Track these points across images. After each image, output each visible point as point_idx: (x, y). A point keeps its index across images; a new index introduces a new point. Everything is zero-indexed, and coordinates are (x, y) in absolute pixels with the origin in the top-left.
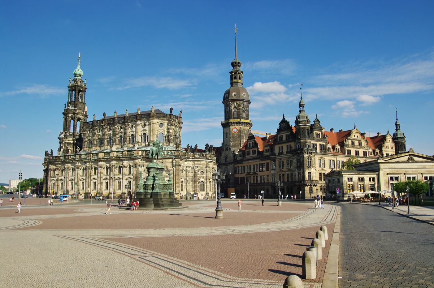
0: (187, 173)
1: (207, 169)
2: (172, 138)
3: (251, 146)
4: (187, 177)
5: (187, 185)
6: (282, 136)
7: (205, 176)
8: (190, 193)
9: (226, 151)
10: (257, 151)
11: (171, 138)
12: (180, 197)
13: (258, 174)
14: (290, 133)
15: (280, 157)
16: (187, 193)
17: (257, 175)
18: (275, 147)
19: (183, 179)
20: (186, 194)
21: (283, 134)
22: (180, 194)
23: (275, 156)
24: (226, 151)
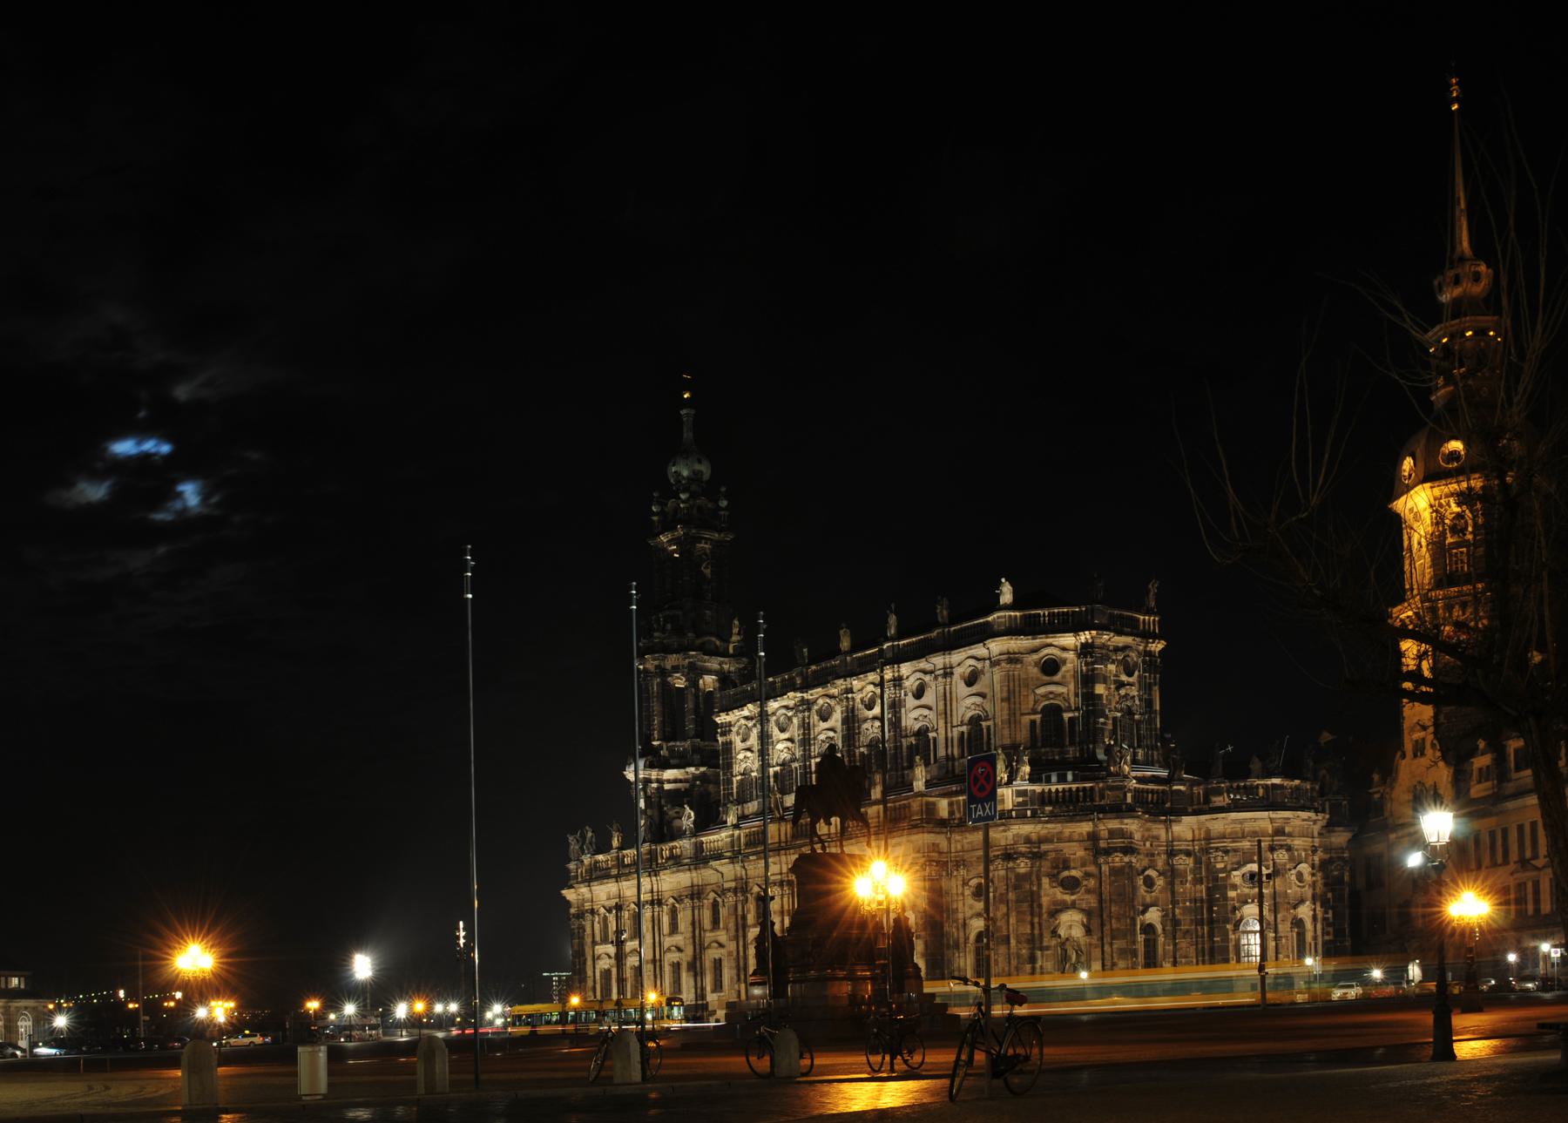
0: (1172, 883)
1: (1281, 856)
4: (1174, 903)
5: (1175, 945)
19: (1153, 916)
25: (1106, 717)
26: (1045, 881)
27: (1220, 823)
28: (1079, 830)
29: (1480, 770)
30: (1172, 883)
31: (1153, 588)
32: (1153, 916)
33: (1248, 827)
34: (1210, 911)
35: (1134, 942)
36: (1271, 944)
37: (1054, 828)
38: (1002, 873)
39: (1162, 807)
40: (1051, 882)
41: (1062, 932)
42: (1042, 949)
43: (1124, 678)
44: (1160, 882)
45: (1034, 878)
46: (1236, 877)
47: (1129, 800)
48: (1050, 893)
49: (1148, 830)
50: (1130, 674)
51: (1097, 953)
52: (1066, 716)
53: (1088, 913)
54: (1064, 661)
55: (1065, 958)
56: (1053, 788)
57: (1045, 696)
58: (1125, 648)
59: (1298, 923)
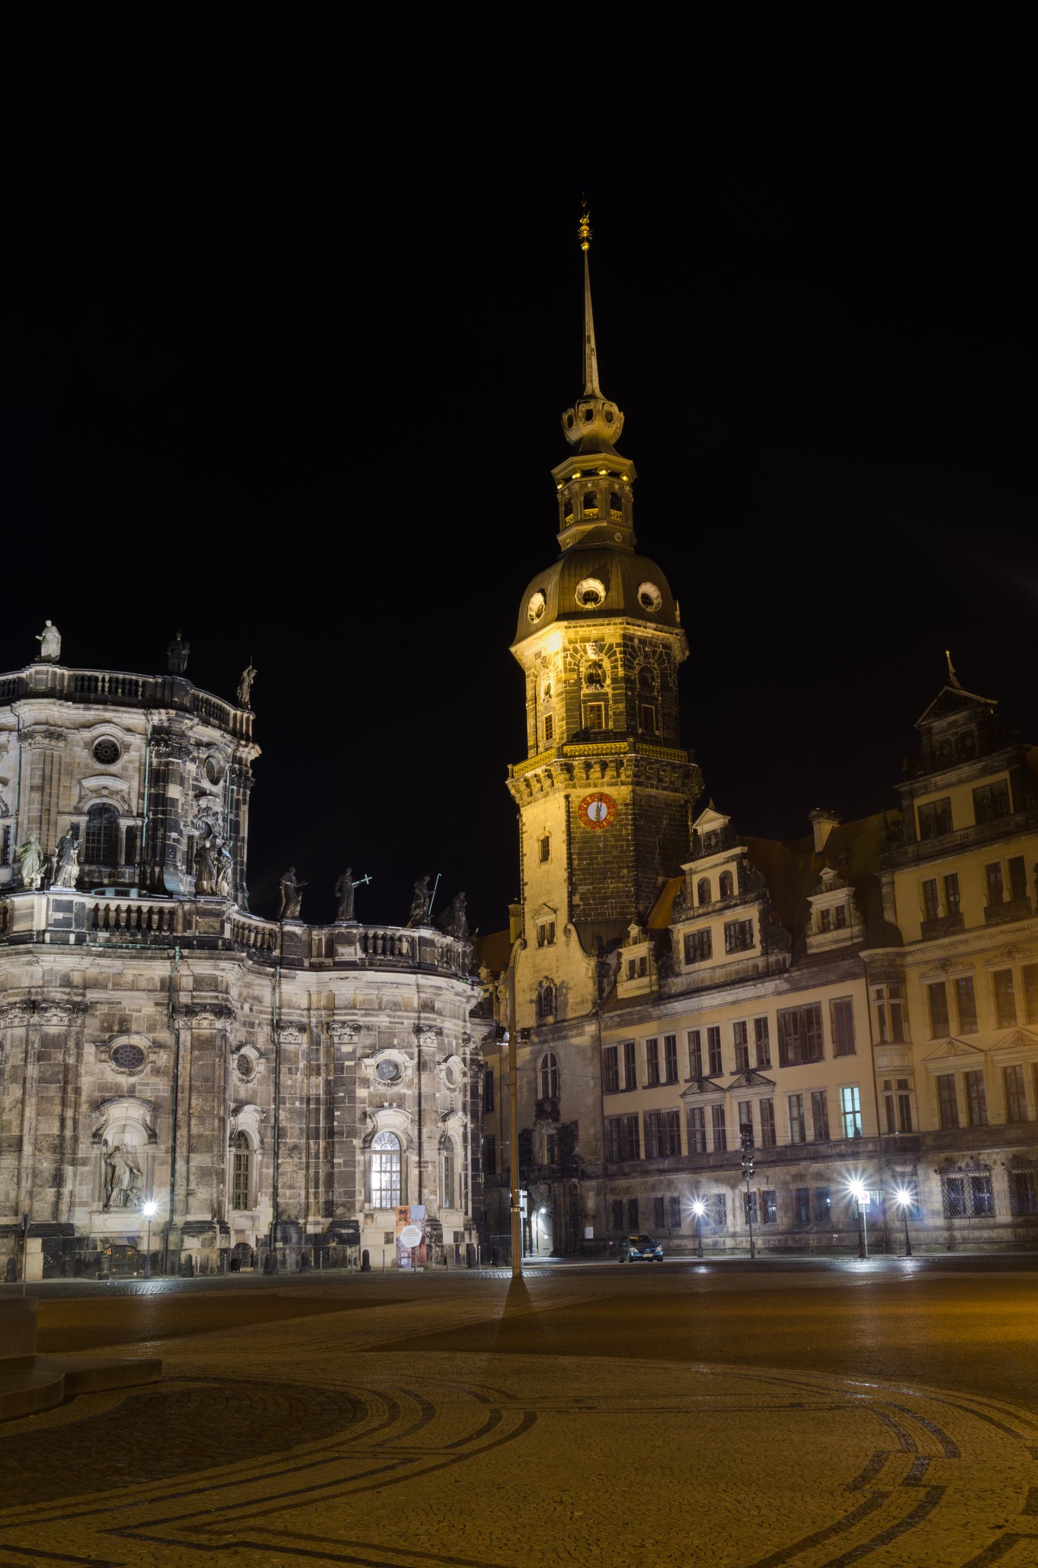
0: (276, 1071)
1: (429, 1042)
2: (185, 841)
3: (715, 894)
4: (278, 1100)
5: (277, 1167)
6: (947, 801)
7: (410, 1092)
8: (301, 1221)
9: (541, 945)
10: (756, 926)
11: (177, 841)
12: (223, 1251)
13: (774, 1084)
14: (1005, 775)
15: (936, 949)
16: (281, 1222)
17: (763, 1092)
18: (893, 883)
19: (248, 1120)
20: (274, 1227)
21: (952, 793)
22: (225, 1230)
23: (901, 944)
24: (541, 945)
25: (181, 834)
26: (89, 1049)
27: (352, 987)
28: (148, 973)
29: (632, 963)
30: (276, 1071)
31: (249, 676)
32: (248, 1120)
33: (389, 995)
34: (330, 1116)
35: (222, 1158)
36: (414, 1172)
37: (110, 966)
38: (20, 1032)
39: (273, 957)
40: (99, 1051)
41: (110, 1135)
42: (74, 1163)
43: (206, 784)
44: (260, 1068)
45: (71, 1043)
46: (369, 1068)
47: (227, 935)
48: (95, 1070)
49: (248, 985)
50: (215, 782)
51: (163, 1172)
52: (124, 823)
53: (155, 1107)
54: (127, 747)
55: (111, 1179)
56: (113, 904)
57: (97, 792)
58: (209, 745)
59: (445, 1142)
